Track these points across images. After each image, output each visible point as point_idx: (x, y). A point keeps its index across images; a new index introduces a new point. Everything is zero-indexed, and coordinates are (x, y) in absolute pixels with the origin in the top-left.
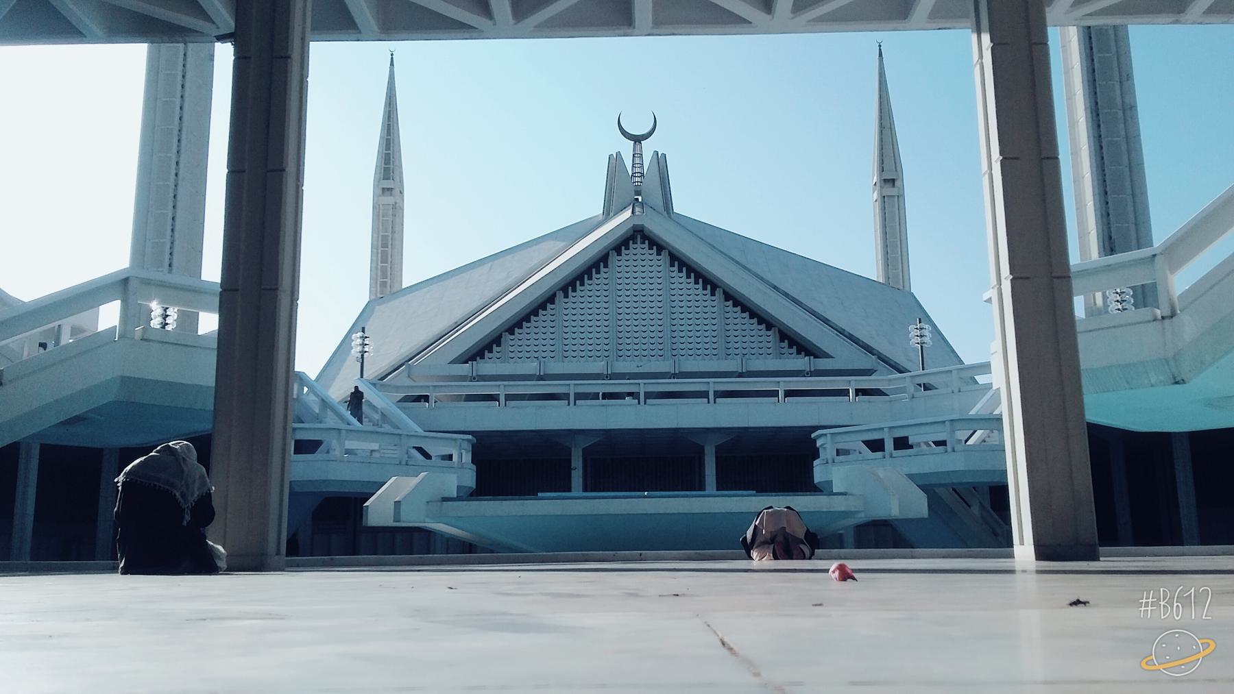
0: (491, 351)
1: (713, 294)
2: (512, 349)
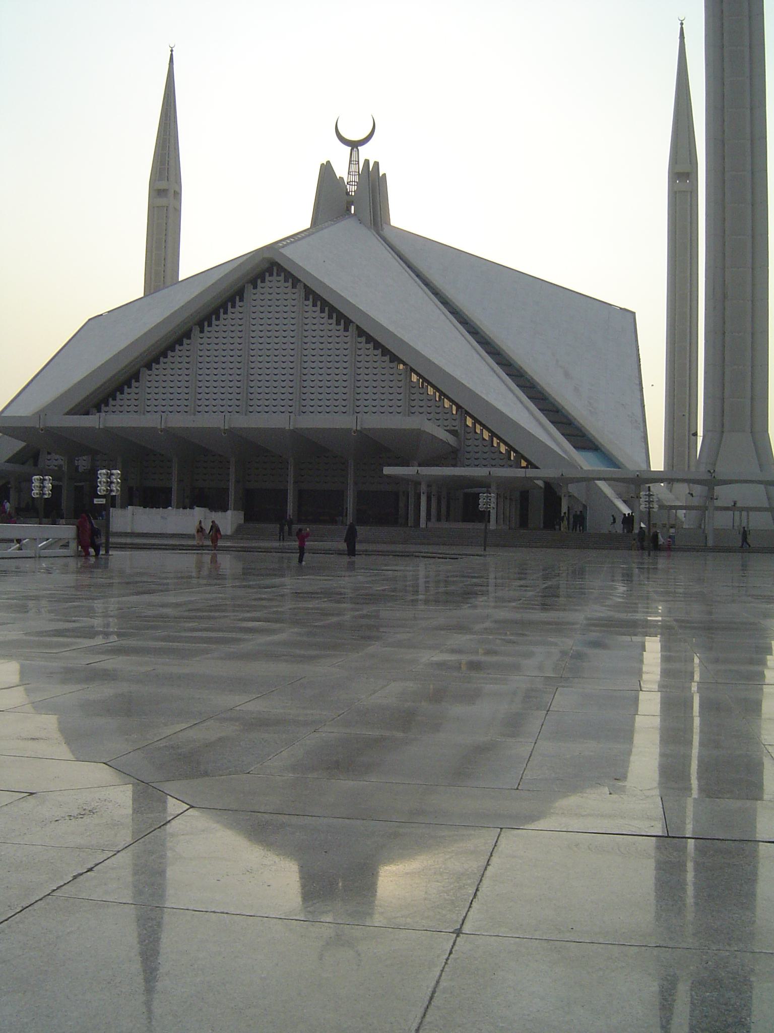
1: (346, 330)
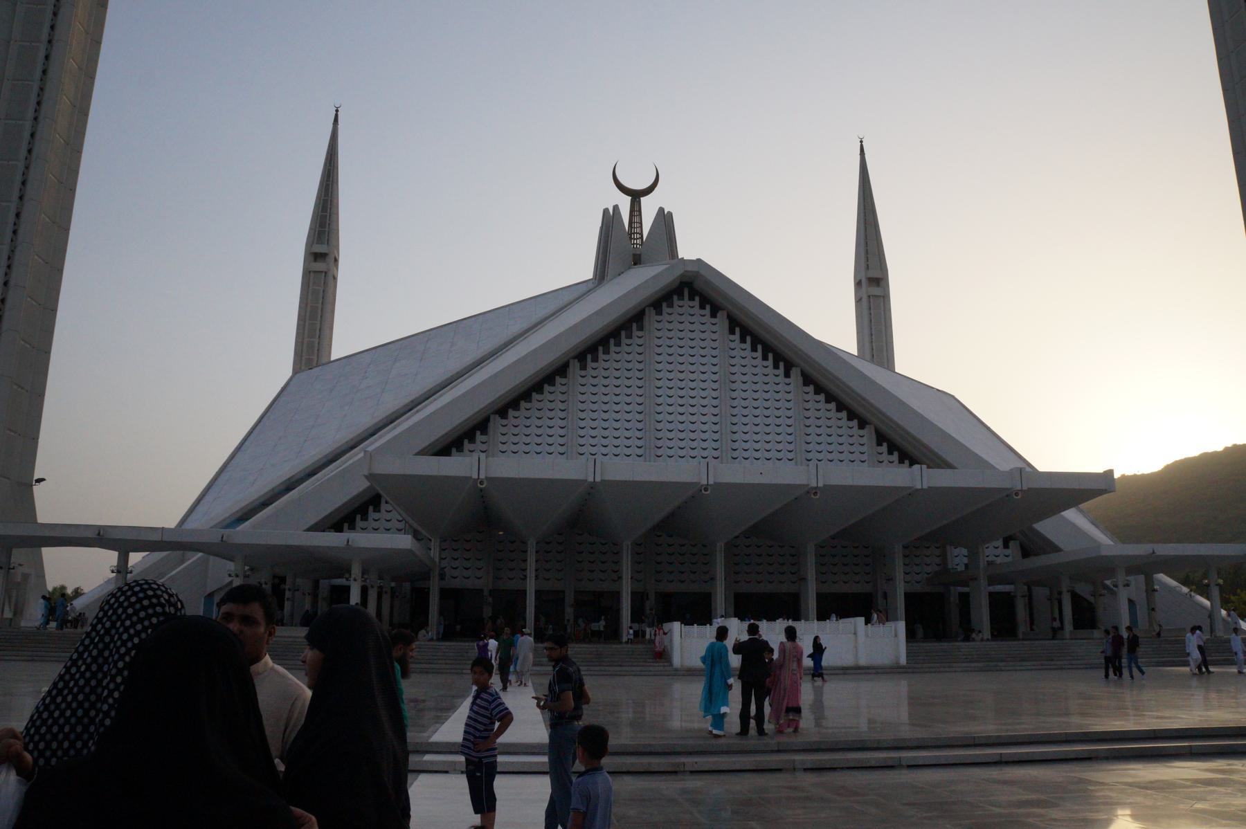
1: (787, 375)
2: (503, 439)
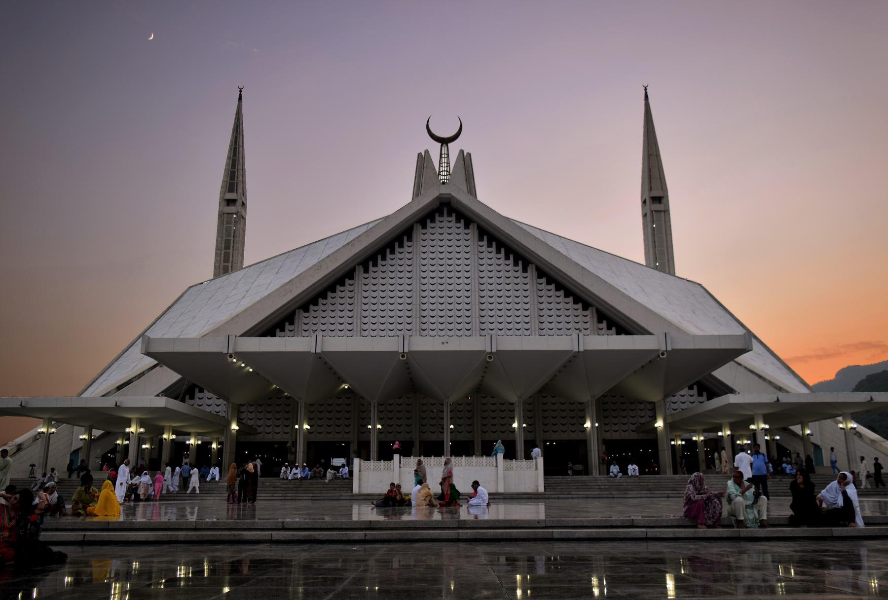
0: (283, 330)
